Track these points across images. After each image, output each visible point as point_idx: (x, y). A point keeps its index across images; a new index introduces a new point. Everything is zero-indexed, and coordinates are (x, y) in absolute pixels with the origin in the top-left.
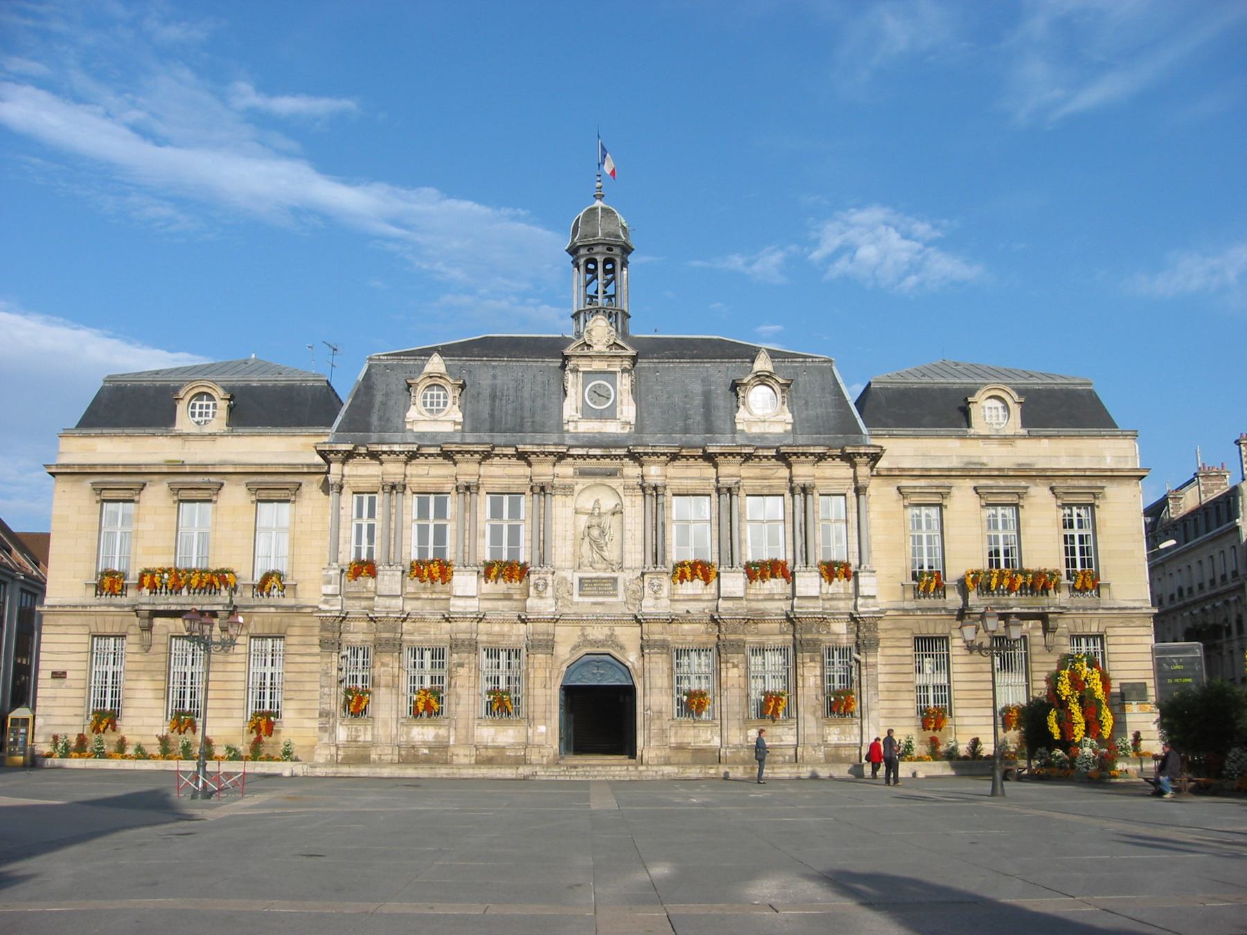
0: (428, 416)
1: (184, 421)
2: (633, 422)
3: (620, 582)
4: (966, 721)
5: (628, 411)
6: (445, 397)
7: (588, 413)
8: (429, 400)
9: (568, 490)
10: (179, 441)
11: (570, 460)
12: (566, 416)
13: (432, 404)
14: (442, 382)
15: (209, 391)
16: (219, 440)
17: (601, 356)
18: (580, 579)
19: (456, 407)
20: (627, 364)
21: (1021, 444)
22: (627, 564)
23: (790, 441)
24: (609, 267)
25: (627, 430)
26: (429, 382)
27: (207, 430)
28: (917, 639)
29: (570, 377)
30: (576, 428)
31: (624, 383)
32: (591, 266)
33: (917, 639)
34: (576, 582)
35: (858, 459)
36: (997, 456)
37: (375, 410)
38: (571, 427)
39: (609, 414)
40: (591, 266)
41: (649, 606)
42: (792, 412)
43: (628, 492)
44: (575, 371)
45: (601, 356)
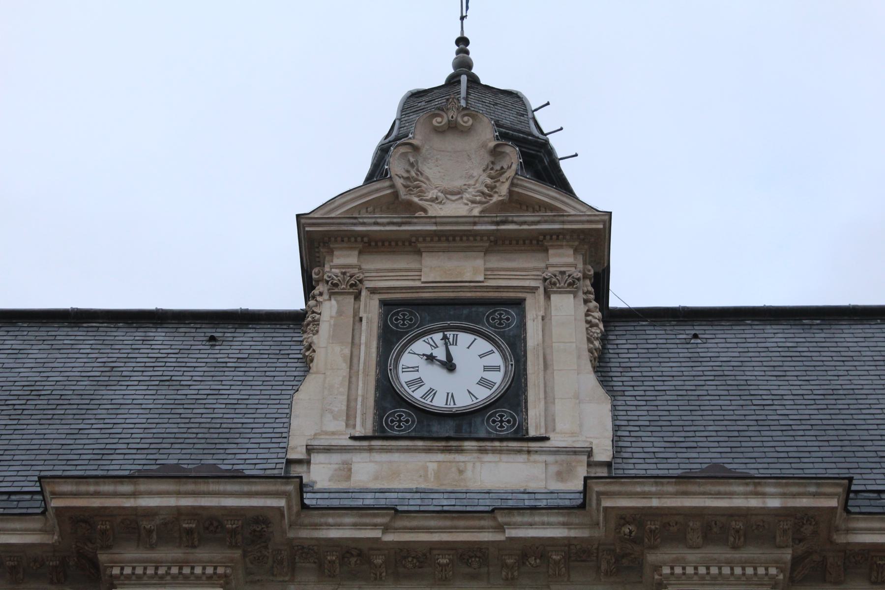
2: (603, 454)
7: (400, 418)
17: (453, 239)
30: (347, 471)
31: (559, 327)
38: (321, 474)
45: (453, 239)
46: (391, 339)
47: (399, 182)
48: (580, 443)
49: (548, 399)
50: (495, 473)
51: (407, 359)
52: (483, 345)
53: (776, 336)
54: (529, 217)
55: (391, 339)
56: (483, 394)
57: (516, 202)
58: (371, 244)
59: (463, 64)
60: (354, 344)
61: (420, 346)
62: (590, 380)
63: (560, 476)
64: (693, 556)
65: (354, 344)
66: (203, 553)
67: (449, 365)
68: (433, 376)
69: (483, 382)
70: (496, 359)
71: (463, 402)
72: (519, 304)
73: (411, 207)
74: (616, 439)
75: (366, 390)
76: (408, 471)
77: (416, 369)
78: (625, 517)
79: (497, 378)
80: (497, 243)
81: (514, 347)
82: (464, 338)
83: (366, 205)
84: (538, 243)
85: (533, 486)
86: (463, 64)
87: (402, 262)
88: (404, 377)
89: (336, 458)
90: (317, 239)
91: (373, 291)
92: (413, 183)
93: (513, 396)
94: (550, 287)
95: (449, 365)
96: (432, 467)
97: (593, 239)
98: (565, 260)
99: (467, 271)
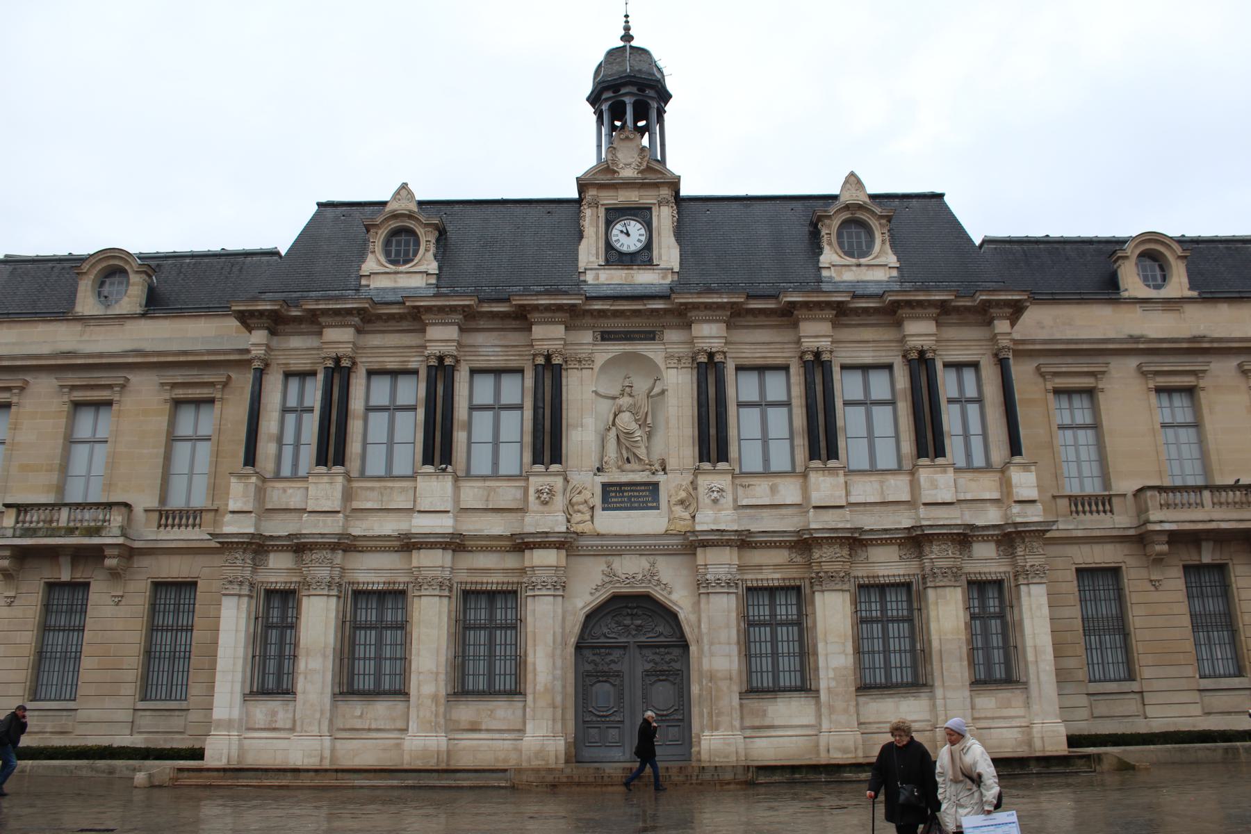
0: (392, 268)
1: (87, 303)
2: (677, 269)
3: (662, 488)
4: (1156, 685)
5: (669, 254)
6: (417, 243)
8: (393, 248)
9: (584, 362)
10: (78, 327)
11: (588, 320)
12: (582, 265)
13: (398, 253)
14: (411, 224)
15: (121, 264)
16: (130, 326)
17: (628, 185)
18: (605, 486)
19: (430, 255)
20: (665, 192)
21: (1191, 311)
22: (672, 463)
23: (897, 287)
24: (642, 123)
25: (668, 280)
26: (394, 224)
27: (117, 310)
28: (1079, 571)
29: (588, 212)
30: (597, 277)
31: (664, 218)
32: (618, 123)
33: (1079, 571)
34: (598, 491)
35: (994, 311)
36: (1158, 326)
38: (589, 277)
39: (643, 258)
40: (618, 123)
41: (707, 520)
42: (895, 253)
43: (673, 362)
44: (595, 204)
45: (628, 185)
46: (609, 224)
49: (660, 248)
50: (644, 278)
51: (615, 232)
52: (639, 226)
53: (735, 205)
54: (653, 176)
55: (609, 224)
56: (639, 245)
57: (649, 169)
58: (601, 186)
59: (627, 37)
60: (597, 226)
61: (619, 227)
62: (673, 240)
63: (663, 278)
64: (701, 314)
65: (597, 226)
66: (557, 315)
67: (628, 234)
68: (623, 238)
69: (639, 241)
70: (643, 231)
71: (633, 249)
72: (650, 209)
73: (615, 172)
74: (681, 264)
75: (602, 244)
76: (615, 278)
78: (681, 304)
79: (643, 238)
80: (643, 186)
81: (648, 225)
82: (633, 223)
84: (656, 185)
85: (655, 282)
86: (627, 37)
87: (611, 193)
88: (614, 239)
90: (583, 185)
92: (614, 162)
93: (648, 246)
94: (660, 204)
95: (628, 234)
97: (675, 184)
98: (665, 192)
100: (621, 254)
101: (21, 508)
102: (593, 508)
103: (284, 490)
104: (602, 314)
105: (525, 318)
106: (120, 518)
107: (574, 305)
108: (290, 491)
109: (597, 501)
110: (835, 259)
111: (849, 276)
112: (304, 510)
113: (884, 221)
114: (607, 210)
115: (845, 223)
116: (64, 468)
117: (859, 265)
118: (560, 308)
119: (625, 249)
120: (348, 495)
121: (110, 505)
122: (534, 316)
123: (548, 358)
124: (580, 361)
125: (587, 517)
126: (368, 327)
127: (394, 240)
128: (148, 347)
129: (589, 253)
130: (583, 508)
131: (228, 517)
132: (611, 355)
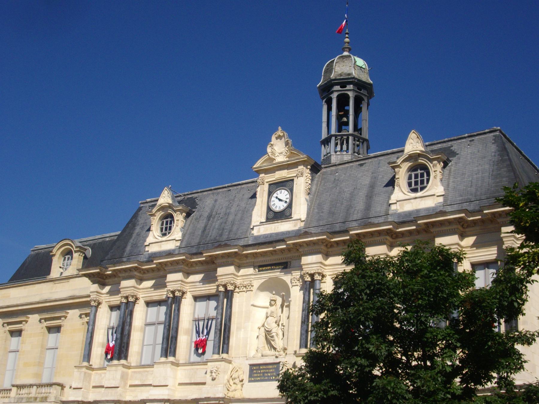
9: (248, 288)
30: (259, 231)
37: (131, 241)
46: (270, 194)
47: (270, 154)
48: (298, 218)
51: (273, 199)
52: (286, 192)
61: (275, 195)
70: (288, 196)
71: (282, 208)
77: (274, 201)
82: (283, 191)
83: (265, 160)
89: (258, 227)
91: (267, 182)
93: (290, 206)
96: (273, 227)
99: (283, 174)
100: (275, 213)
101: (20, 387)
102: (242, 381)
103: (100, 375)
104: (255, 255)
105: (213, 263)
106: (55, 392)
107: (236, 253)
108: (103, 375)
109: (246, 376)
110: (401, 196)
111: (408, 207)
112: (102, 387)
113: (435, 162)
114: (270, 185)
115: (412, 169)
116: (41, 364)
117: (416, 198)
118: (229, 255)
119: (277, 210)
120: (124, 377)
121: (51, 385)
122: (218, 261)
123: (225, 286)
124: (246, 287)
125: (239, 386)
126: (145, 276)
127: (165, 221)
128: (78, 293)
129: (258, 214)
130: (237, 381)
131: (71, 391)
132: (263, 280)
